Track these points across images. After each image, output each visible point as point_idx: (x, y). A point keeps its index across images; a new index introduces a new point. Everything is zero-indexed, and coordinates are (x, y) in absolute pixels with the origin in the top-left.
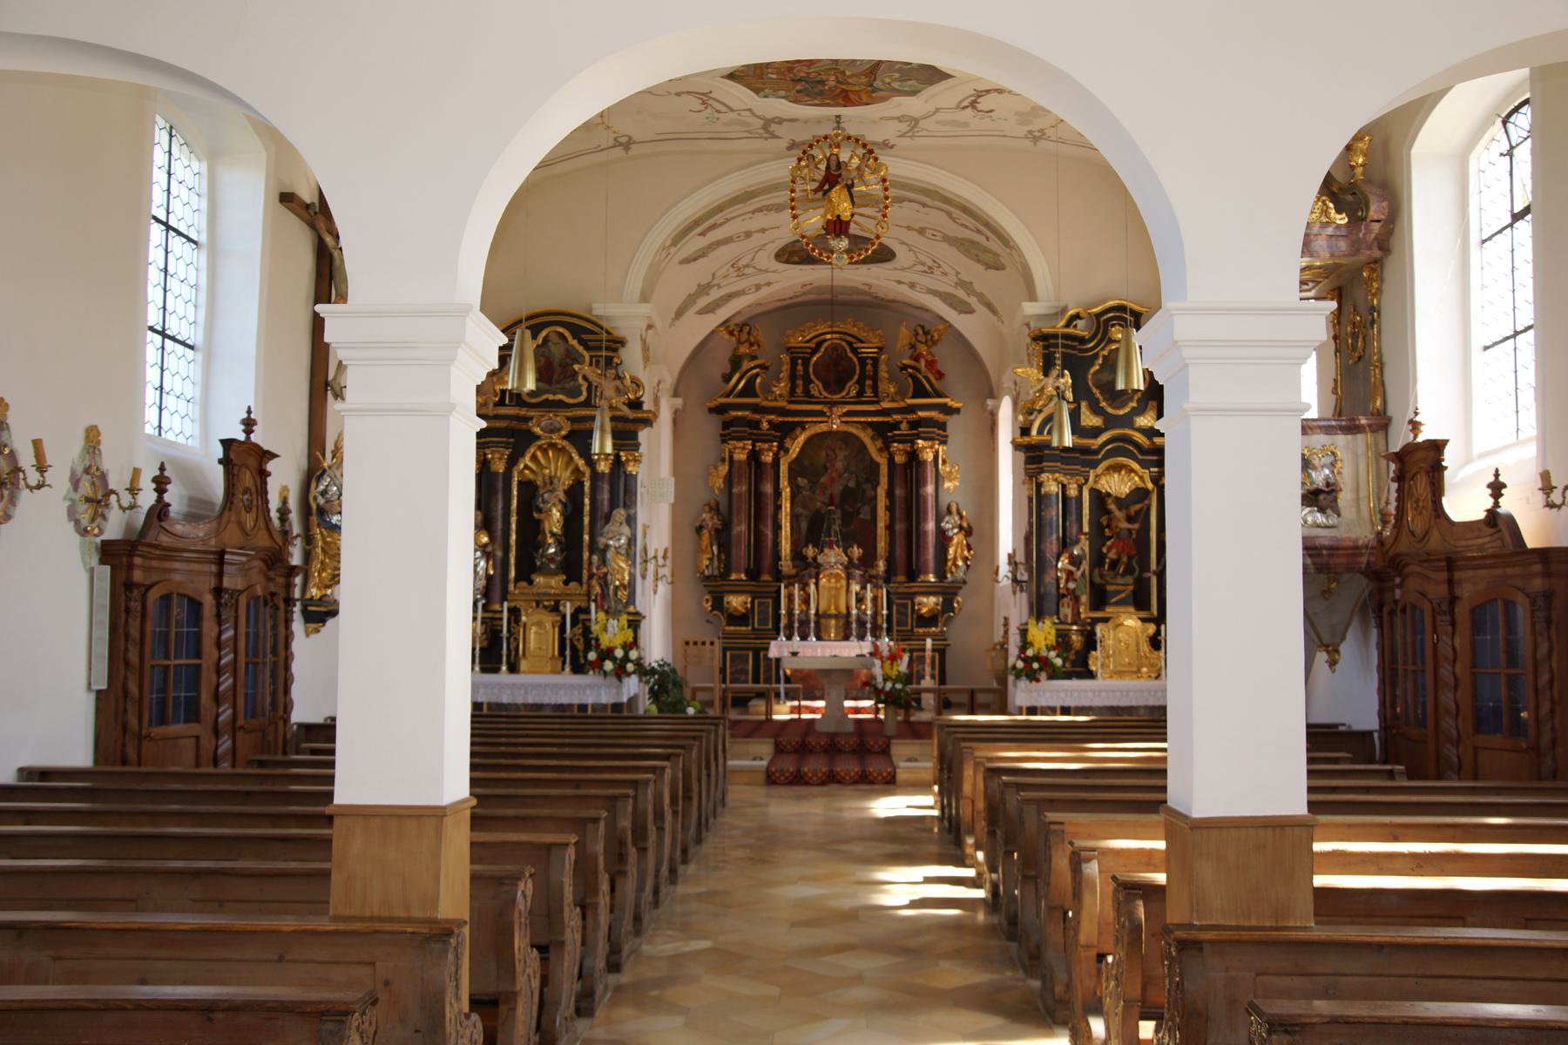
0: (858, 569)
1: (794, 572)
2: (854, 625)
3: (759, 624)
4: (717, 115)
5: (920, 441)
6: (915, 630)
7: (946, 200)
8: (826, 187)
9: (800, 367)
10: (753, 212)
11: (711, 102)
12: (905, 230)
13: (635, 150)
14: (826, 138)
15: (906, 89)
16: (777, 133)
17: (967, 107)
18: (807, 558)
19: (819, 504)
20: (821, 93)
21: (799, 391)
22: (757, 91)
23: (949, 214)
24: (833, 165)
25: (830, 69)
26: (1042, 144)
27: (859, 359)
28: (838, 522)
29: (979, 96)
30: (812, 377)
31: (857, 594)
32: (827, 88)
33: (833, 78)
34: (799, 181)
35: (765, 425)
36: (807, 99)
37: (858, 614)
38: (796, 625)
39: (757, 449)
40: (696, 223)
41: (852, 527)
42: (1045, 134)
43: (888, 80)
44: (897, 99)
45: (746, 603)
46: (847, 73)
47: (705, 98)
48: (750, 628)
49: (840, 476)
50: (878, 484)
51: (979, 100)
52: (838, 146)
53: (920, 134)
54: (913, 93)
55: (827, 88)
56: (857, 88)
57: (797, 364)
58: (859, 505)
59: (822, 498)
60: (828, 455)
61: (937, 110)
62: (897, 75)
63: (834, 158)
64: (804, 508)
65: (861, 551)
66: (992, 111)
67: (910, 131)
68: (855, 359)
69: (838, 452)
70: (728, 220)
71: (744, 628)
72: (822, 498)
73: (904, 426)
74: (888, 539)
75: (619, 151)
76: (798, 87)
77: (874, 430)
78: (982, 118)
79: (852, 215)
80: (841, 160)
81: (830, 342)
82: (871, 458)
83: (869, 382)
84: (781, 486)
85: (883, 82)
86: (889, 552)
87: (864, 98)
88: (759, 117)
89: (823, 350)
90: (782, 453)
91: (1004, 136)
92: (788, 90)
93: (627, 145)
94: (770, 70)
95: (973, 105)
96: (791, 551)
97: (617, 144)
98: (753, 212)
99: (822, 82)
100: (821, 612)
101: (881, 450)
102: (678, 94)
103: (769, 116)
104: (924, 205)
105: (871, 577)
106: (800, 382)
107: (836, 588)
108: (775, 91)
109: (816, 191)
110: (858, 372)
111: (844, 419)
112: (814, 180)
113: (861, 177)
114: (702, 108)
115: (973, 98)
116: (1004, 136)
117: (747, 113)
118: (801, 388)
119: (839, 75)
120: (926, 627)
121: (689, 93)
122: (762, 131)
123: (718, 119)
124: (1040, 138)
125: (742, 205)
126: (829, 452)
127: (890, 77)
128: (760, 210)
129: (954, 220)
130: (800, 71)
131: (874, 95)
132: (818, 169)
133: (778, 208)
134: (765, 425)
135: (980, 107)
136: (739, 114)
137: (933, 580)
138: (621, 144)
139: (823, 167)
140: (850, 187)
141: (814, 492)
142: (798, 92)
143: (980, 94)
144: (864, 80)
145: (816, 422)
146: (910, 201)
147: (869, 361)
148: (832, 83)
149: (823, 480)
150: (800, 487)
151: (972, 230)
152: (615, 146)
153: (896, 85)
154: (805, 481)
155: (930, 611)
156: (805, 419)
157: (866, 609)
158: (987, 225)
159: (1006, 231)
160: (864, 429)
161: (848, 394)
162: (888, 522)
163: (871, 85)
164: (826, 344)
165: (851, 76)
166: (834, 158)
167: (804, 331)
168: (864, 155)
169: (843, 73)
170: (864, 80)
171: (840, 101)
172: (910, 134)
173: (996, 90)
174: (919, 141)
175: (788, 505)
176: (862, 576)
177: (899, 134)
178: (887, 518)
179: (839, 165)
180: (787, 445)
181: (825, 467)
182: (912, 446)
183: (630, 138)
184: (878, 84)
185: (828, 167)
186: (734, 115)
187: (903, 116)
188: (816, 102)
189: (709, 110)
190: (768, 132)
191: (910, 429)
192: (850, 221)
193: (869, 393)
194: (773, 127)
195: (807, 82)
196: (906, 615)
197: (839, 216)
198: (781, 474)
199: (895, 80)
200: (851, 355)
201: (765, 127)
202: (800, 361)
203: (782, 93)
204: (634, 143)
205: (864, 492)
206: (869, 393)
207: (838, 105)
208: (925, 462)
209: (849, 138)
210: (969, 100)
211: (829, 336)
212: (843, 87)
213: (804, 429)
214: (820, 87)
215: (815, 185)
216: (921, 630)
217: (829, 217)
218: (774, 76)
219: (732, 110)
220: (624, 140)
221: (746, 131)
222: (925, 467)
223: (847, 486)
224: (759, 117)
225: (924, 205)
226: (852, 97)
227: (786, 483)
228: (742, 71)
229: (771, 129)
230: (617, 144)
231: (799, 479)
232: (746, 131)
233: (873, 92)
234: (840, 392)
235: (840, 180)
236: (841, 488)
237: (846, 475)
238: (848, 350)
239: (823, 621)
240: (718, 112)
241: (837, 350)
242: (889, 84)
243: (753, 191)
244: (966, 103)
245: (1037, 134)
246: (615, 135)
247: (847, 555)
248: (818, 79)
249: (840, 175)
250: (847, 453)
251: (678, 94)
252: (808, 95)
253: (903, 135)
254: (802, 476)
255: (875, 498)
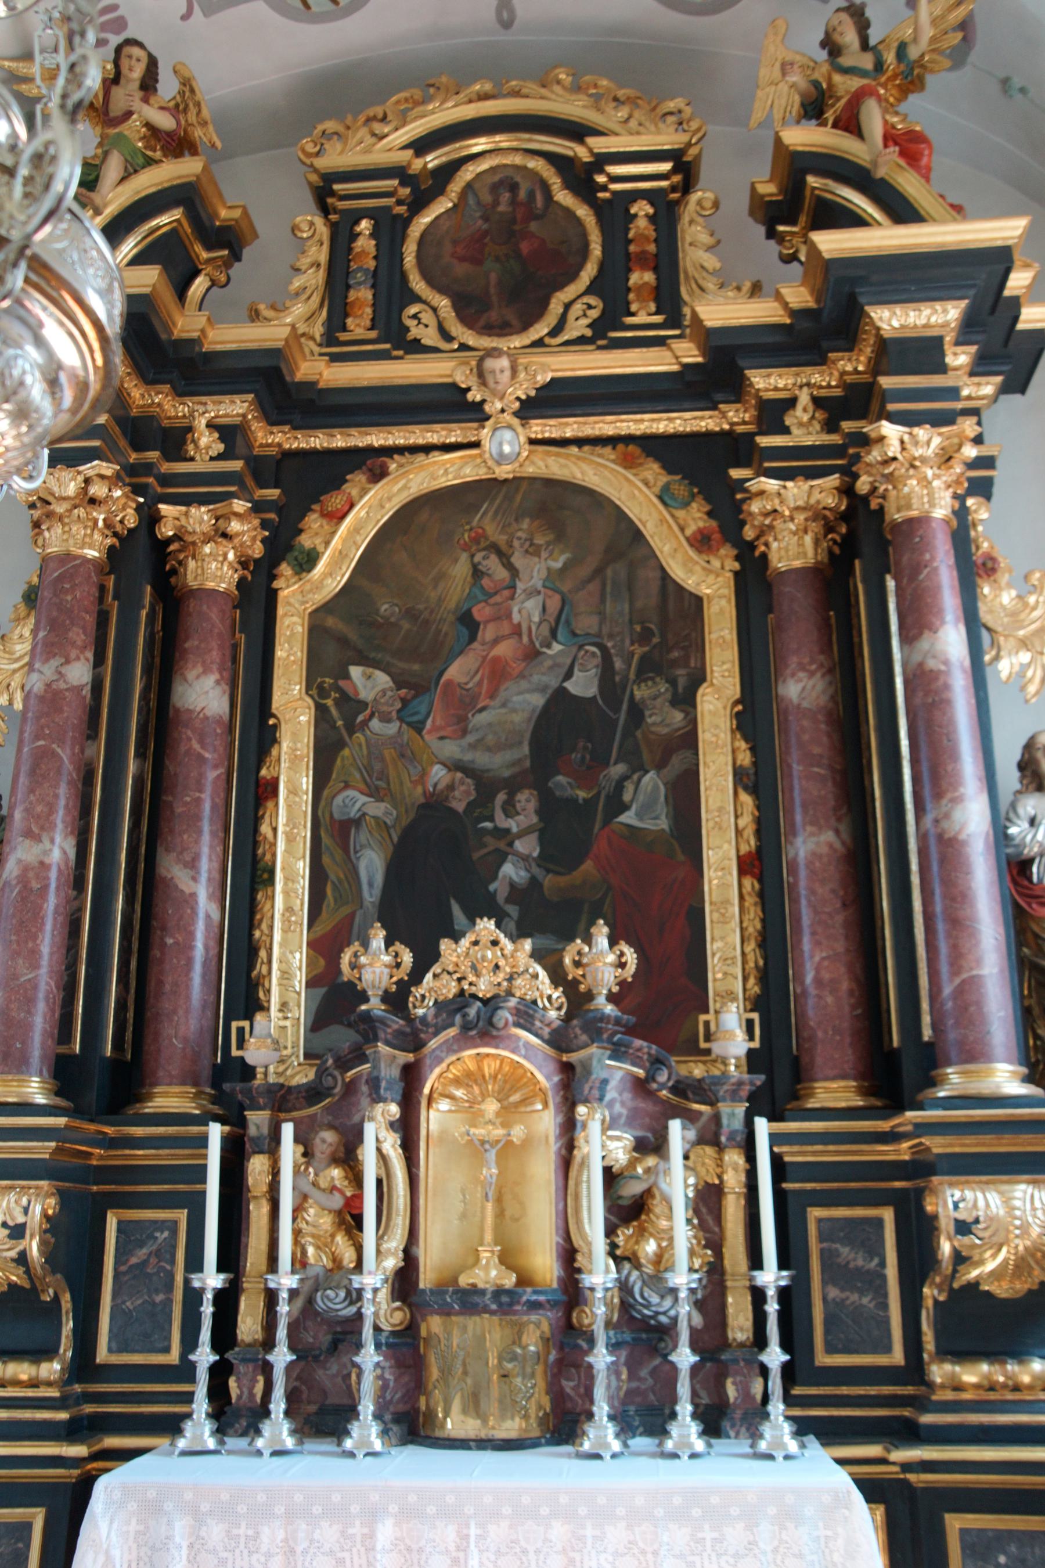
0: (618, 1052)
1: (302, 1076)
2: (601, 1358)
3: (120, 1344)
5: (890, 430)
6: (939, 1372)
9: (365, 243)
18: (363, 997)
19: (438, 774)
21: (358, 326)
27: (599, 209)
28: (528, 846)
30: (418, 284)
31: (611, 1177)
35: (207, 441)
37: (624, 1287)
38: (281, 1357)
39: (167, 530)
41: (588, 866)
45: (17, 1232)
48: (52, 1369)
49: (532, 655)
50: (699, 678)
57: (354, 236)
58: (618, 770)
59: (451, 749)
60: (477, 573)
64: (374, 793)
65: (631, 956)
68: (583, 212)
69: (518, 560)
71: (23, 1370)
72: (451, 749)
73: (801, 414)
74: (754, 914)
77: (669, 467)
81: (484, 165)
82: (665, 576)
83: (641, 278)
84: (278, 701)
86: (764, 976)
89: (455, 187)
90: (285, 569)
96: (308, 985)
100: (426, 1280)
101: (702, 542)
105: (683, 1089)
106: (362, 294)
107: (507, 1150)
110: (596, 250)
111: (540, 428)
118: (369, 310)
120: (995, 1354)
126: (493, 564)
134: (207, 441)
137: (1016, 1088)
141: (418, 727)
145: (427, 449)
147: (642, 209)
149: (456, 671)
150: (364, 705)
154: (382, 679)
155: (1021, 1265)
156: (377, 438)
157: (662, 1261)
160: (628, 462)
161: (555, 332)
162: (750, 843)
164: (468, 173)
167: (384, 119)
175: (306, 783)
176: (641, 1087)
178: (747, 821)
180: (306, 540)
181: (469, 624)
182: (847, 490)
191: (830, 427)
193: (644, 314)
196: (876, 1283)
198: (280, 653)
200: (564, 197)
202: (365, 225)
205: (637, 713)
206: (644, 314)
208: (916, 525)
211: (479, 144)
213: (378, 475)
216: (972, 1374)
222: (926, 545)
223: (560, 696)
227: (297, 689)
231: (356, 672)
234: (526, 326)
236: (538, 700)
237: (557, 647)
238: (555, 182)
239: (434, 1324)
241: (514, 187)
247: (558, 977)
250: (558, 565)
254: (363, 660)
255: (689, 739)
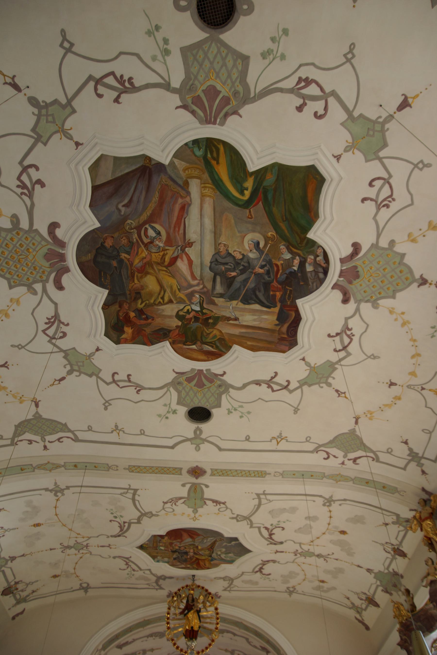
4: (133, 572)
7: (246, 628)
8: (186, 611)
10: (148, 636)
11: (130, 564)
12: (224, 652)
13: (91, 593)
14: (187, 586)
15: (228, 559)
16: (162, 586)
17: (257, 572)
20: (185, 561)
22: (154, 557)
23: (247, 640)
24: (190, 599)
25: (191, 545)
26: (294, 596)
29: (264, 565)
32: (189, 557)
33: (192, 551)
34: (172, 609)
36: (178, 564)
40: (117, 637)
42: (295, 589)
43: (219, 553)
44: (223, 566)
46: (200, 548)
47: (128, 561)
51: (264, 567)
52: (193, 590)
53: (234, 589)
54: (231, 562)
55: (189, 557)
56: (203, 558)
61: (243, 573)
62: (224, 550)
63: (191, 596)
66: (270, 574)
67: (228, 587)
70: (134, 640)
75: (81, 593)
76: (175, 556)
78: (265, 579)
79: (200, 627)
80: (194, 597)
85: (217, 554)
87: (207, 565)
88: (154, 575)
91: (275, 591)
92: (169, 558)
93: (86, 588)
94: (161, 544)
95: (260, 570)
97: (82, 588)
98: (148, 636)
99: (186, 553)
102: (114, 558)
103: (159, 574)
104: (235, 634)
108: (163, 558)
109: (181, 613)
112: (180, 608)
113: (205, 607)
114: (125, 567)
115: (261, 566)
116: (275, 591)
117: (148, 572)
119: (195, 549)
121: (120, 557)
122: (155, 584)
123: (133, 575)
124: (293, 592)
125: (141, 629)
127: (220, 551)
128: (151, 635)
129: (249, 643)
130: (176, 545)
131: (212, 562)
132: (182, 602)
133: (161, 635)
135: (264, 571)
136: (144, 573)
138: (83, 588)
139: (185, 601)
140: (198, 612)
142: (175, 559)
143: (265, 563)
144: (207, 552)
146: (228, 632)
148: (191, 554)
151: (259, 649)
152: (80, 589)
153: (223, 556)
158: (268, 642)
159: (277, 643)
163: (211, 556)
165: (202, 550)
166: (191, 596)
168: (206, 595)
169: (197, 547)
170: (207, 552)
171: (195, 566)
172: (229, 589)
173: (272, 561)
174: (234, 594)
177: (224, 588)
179: (193, 600)
183: (88, 585)
184: (214, 555)
185: (188, 601)
186: (141, 573)
187: (226, 577)
188: (183, 566)
189: (129, 569)
190: (158, 585)
192: (198, 631)
194: (161, 582)
195: (179, 553)
197: (192, 627)
199: (222, 553)
201: (157, 582)
203: (166, 559)
204: (90, 588)
207: (193, 568)
209: (199, 586)
210: (258, 567)
212: (197, 556)
214: (185, 556)
215: (181, 610)
217: (187, 627)
218: (162, 548)
219: (141, 569)
220: (85, 585)
221: (147, 584)
224: (154, 575)
225: (235, 634)
226: (201, 563)
228: (147, 544)
229: (160, 583)
230: (82, 588)
232: (147, 584)
233: (212, 560)
235: (193, 607)
240: (134, 570)
242: (220, 555)
243: (148, 620)
244: (257, 569)
245: (291, 589)
246: (81, 582)
248: (185, 551)
249: (194, 605)
251: (114, 558)
252: (179, 562)
253: (225, 590)
